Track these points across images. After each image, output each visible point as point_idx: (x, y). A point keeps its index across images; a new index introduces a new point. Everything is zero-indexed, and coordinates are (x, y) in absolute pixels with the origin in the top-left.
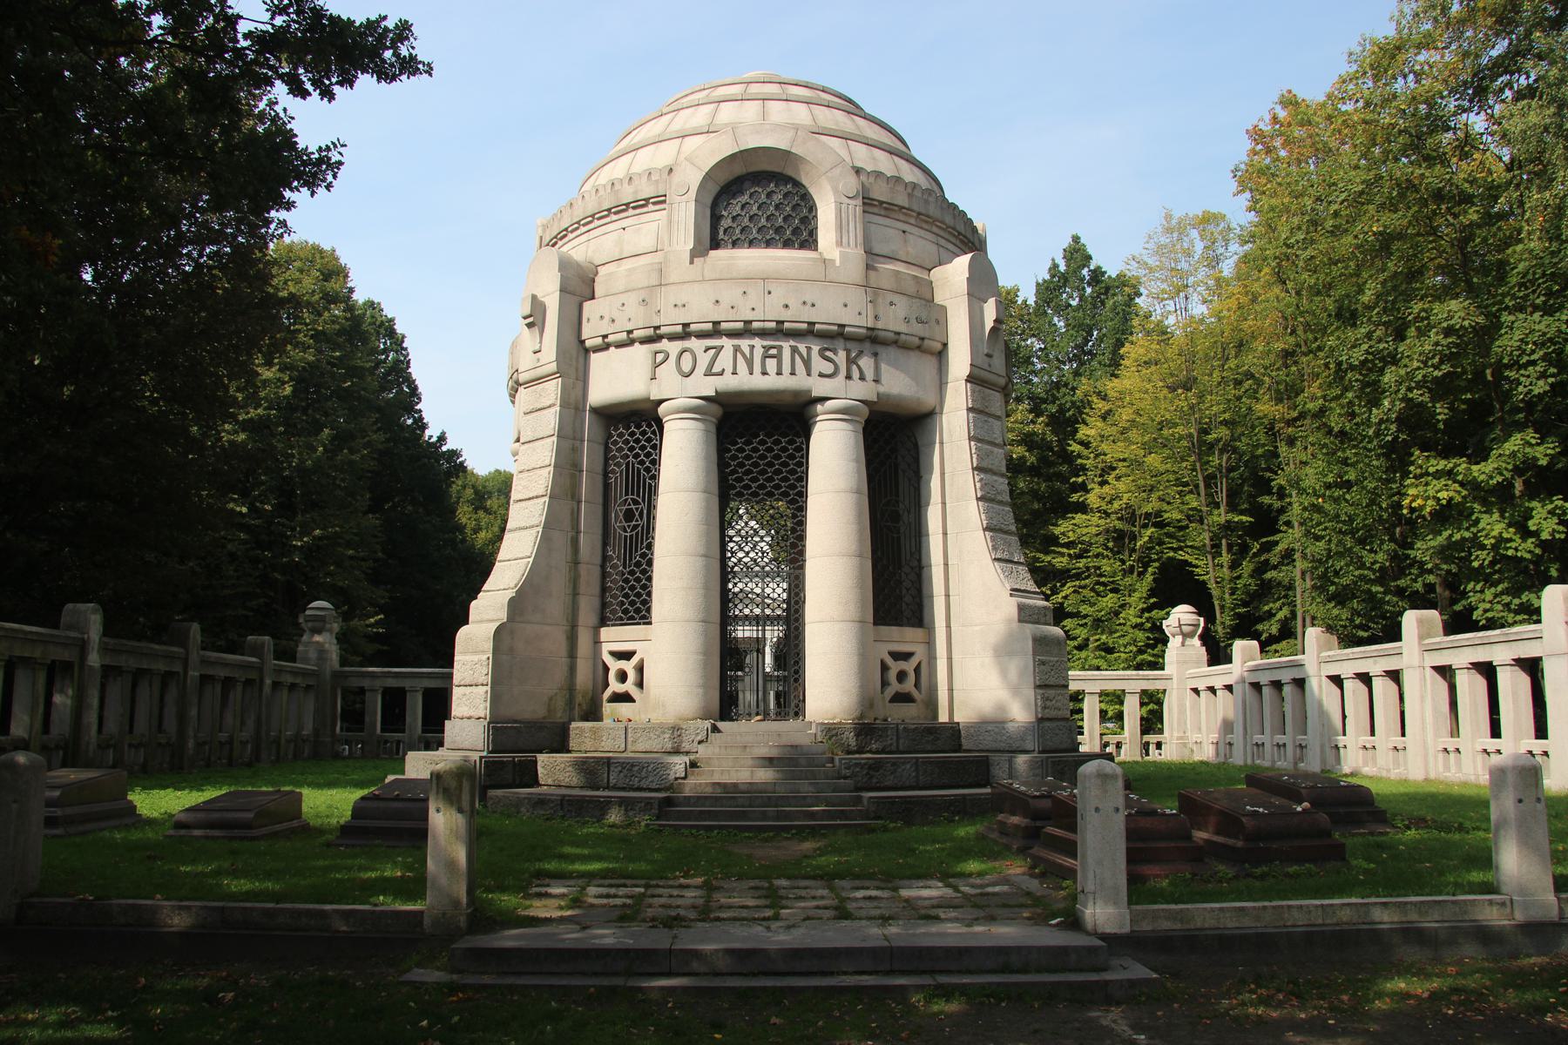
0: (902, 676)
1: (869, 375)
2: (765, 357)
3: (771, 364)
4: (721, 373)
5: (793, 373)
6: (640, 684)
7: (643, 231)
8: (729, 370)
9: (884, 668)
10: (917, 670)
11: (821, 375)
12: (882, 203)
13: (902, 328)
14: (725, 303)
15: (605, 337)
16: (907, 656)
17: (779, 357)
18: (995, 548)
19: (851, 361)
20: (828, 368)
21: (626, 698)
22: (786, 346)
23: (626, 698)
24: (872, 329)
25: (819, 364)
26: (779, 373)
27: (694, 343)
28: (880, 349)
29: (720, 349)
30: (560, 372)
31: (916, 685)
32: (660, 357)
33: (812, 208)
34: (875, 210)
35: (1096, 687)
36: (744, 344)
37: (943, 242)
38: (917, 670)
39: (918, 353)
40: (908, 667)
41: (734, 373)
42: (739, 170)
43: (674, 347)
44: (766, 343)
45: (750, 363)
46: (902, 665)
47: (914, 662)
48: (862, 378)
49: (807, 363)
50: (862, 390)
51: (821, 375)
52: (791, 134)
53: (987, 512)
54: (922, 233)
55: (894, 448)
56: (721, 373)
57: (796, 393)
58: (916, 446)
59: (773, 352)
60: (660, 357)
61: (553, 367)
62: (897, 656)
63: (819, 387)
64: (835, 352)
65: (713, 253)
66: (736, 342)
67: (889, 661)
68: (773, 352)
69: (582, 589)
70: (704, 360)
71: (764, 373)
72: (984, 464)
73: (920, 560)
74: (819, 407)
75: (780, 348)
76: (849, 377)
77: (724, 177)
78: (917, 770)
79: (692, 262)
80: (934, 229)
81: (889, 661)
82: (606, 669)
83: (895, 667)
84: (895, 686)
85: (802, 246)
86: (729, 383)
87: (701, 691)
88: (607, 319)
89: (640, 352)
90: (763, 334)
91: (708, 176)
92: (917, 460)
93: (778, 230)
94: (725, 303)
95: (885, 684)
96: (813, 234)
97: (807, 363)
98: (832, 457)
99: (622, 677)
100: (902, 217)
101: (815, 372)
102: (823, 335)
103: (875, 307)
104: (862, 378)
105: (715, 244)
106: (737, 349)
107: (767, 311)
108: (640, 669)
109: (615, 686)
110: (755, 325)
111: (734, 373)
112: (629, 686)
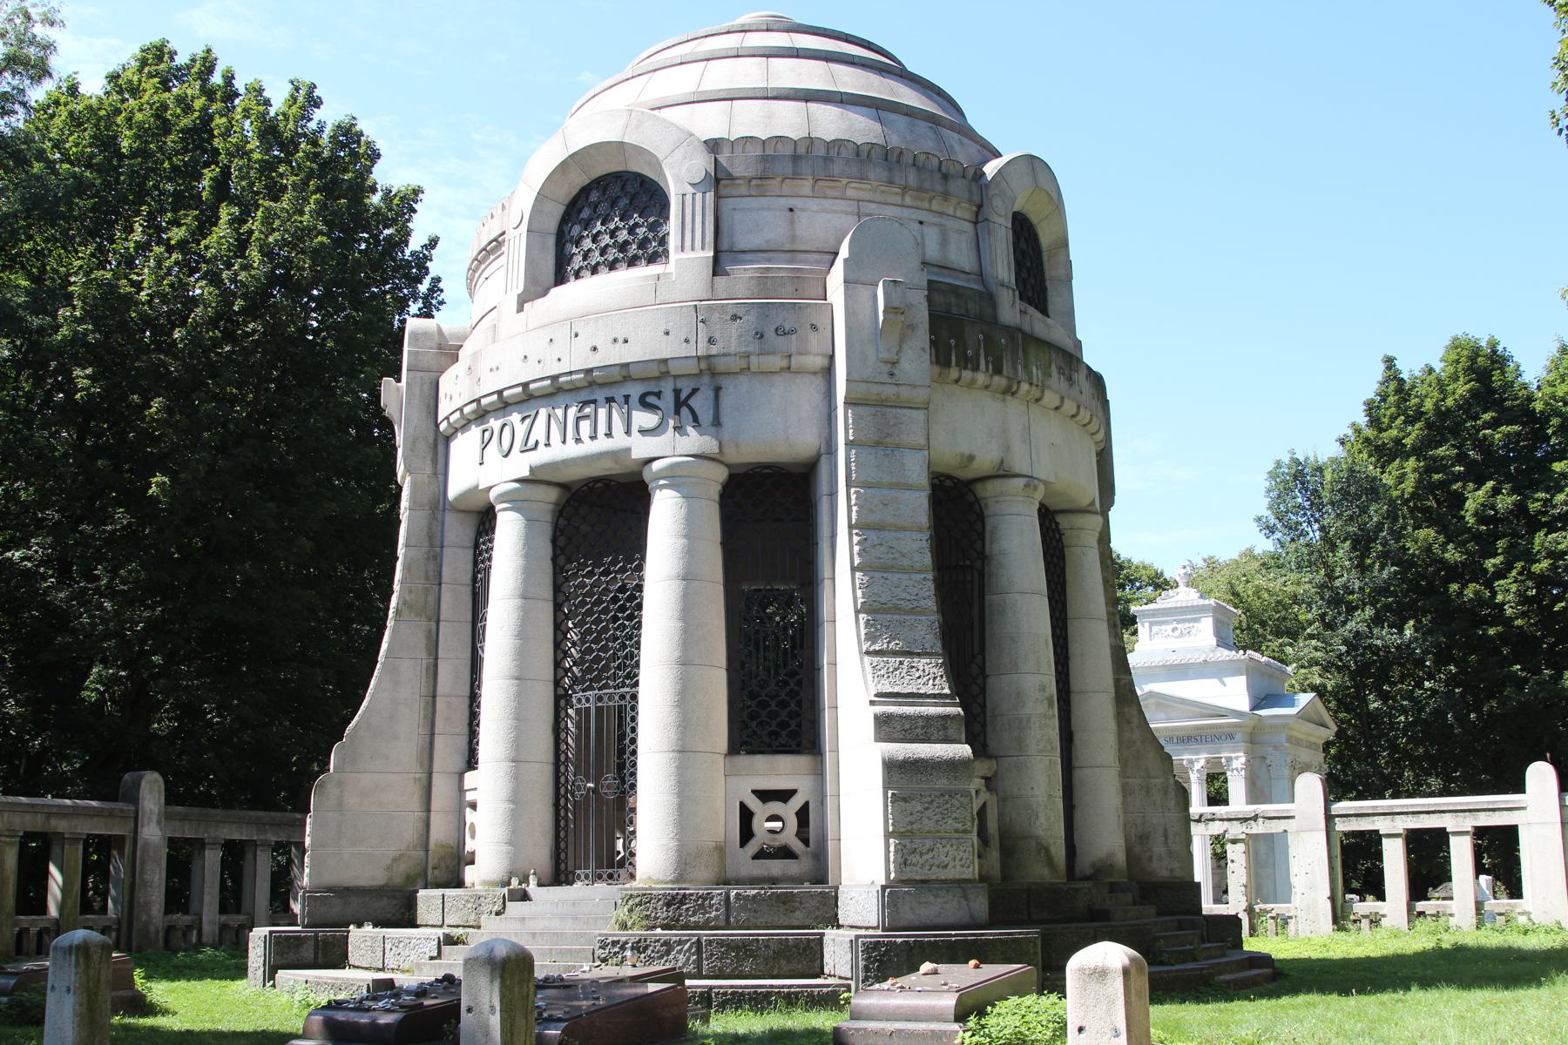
1: (706, 416)
3: (585, 426)
5: (609, 435)
8: (542, 441)
9: (746, 815)
11: (643, 432)
14: (532, 360)
16: (785, 796)
18: (871, 637)
24: (709, 357)
32: (487, 434)
35: (1468, 823)
38: (803, 814)
39: (787, 375)
42: (579, 180)
43: (495, 424)
47: (796, 803)
51: (643, 432)
53: (866, 587)
54: (827, 203)
55: (767, 518)
60: (487, 434)
62: (765, 796)
63: (641, 447)
64: (658, 395)
65: (555, 291)
67: (754, 804)
69: (439, 726)
70: (521, 430)
71: (578, 440)
72: (875, 518)
78: (699, 952)
79: (520, 309)
81: (754, 804)
85: (652, 259)
87: (505, 848)
89: (475, 432)
91: (541, 196)
93: (623, 247)
95: (746, 834)
96: (663, 241)
101: (635, 428)
102: (574, 389)
105: (560, 279)
107: (573, 359)
111: (547, 445)
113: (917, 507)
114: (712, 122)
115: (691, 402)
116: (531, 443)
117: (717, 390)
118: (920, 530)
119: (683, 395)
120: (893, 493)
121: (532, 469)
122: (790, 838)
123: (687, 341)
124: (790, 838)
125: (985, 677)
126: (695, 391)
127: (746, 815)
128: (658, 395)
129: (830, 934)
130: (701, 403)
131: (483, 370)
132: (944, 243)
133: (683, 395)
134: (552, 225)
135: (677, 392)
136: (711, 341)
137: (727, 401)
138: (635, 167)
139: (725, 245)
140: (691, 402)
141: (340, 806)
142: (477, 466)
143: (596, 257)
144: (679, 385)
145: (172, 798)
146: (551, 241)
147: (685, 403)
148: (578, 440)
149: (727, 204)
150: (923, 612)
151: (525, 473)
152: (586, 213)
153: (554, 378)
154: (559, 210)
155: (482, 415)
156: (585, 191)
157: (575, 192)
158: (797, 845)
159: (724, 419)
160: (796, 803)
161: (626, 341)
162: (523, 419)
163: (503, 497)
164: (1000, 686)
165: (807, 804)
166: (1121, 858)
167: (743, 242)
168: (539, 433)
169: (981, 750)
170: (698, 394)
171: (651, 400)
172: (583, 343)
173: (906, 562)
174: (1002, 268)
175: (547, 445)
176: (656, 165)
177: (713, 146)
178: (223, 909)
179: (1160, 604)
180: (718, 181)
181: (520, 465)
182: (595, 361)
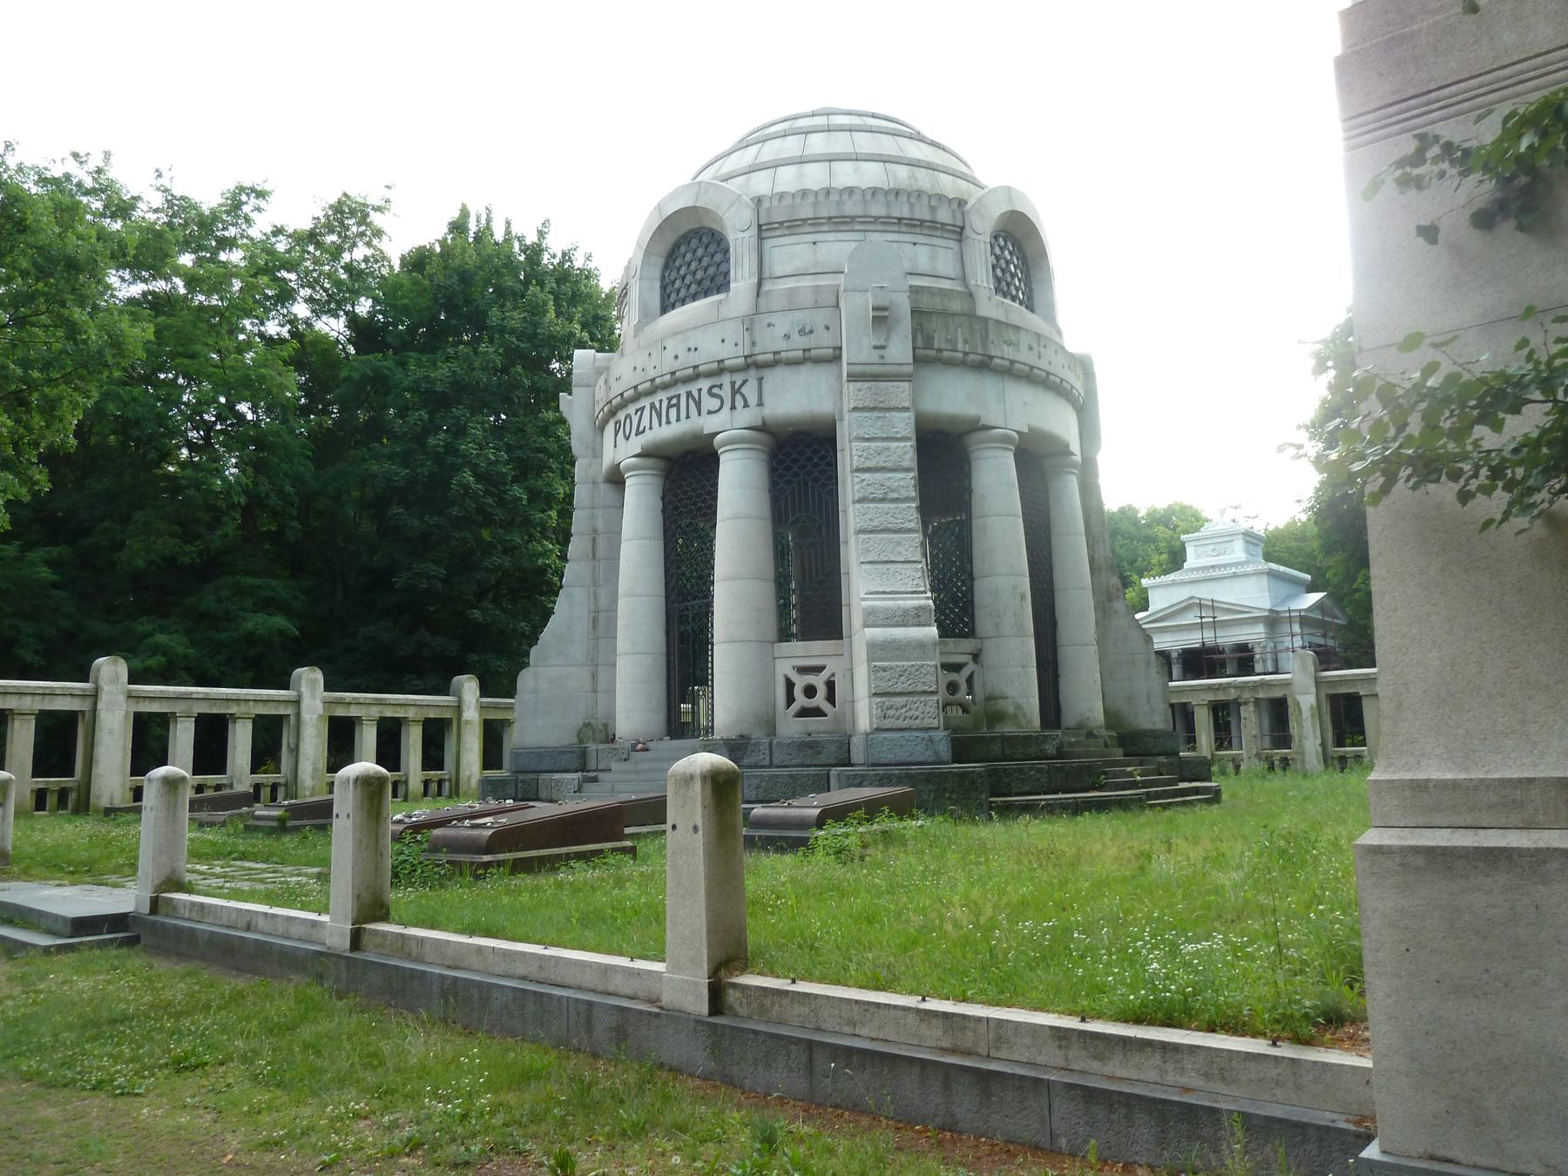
0: (810, 691)
3: (673, 411)
9: (790, 685)
11: (710, 412)
12: (781, 223)
13: (781, 345)
14: (639, 369)
17: (678, 405)
20: (715, 403)
22: (682, 390)
25: (709, 403)
26: (678, 420)
28: (767, 373)
31: (831, 698)
34: (778, 233)
42: (671, 238)
43: (621, 416)
48: (746, 405)
50: (746, 417)
51: (710, 412)
54: (840, 236)
59: (674, 401)
63: (709, 424)
64: (720, 386)
67: (795, 677)
68: (674, 401)
70: (635, 420)
71: (668, 422)
76: (733, 407)
77: (663, 248)
80: (858, 227)
84: (801, 700)
86: (649, 437)
90: (665, 387)
93: (700, 283)
94: (639, 369)
95: (790, 699)
97: (698, 405)
98: (738, 487)
101: (704, 411)
104: (746, 405)
110: (658, 381)
113: (905, 452)
114: (761, 184)
117: (761, 380)
118: (907, 470)
120: (882, 444)
122: (819, 700)
124: (819, 700)
125: (972, 579)
126: (745, 381)
127: (790, 685)
128: (720, 386)
129: (834, 771)
130: (750, 391)
131: (612, 381)
132: (933, 258)
134: (657, 274)
135: (733, 384)
136: (753, 344)
137: (767, 387)
139: (766, 274)
141: (535, 690)
142: (620, 450)
143: (683, 293)
145: (485, 691)
146: (657, 285)
148: (668, 422)
149: (768, 244)
150: (909, 531)
152: (677, 264)
153: (653, 380)
154: (660, 262)
155: (613, 413)
156: (677, 246)
157: (669, 247)
158: (826, 706)
159: (766, 400)
160: (825, 675)
164: (984, 589)
166: (1099, 716)
167: (779, 270)
168: (645, 422)
169: (945, 632)
171: (715, 390)
172: (669, 354)
173: (895, 495)
174: (982, 278)
176: (719, 220)
177: (759, 201)
178: (487, 765)
180: (763, 231)
181: (636, 444)
182: (676, 365)
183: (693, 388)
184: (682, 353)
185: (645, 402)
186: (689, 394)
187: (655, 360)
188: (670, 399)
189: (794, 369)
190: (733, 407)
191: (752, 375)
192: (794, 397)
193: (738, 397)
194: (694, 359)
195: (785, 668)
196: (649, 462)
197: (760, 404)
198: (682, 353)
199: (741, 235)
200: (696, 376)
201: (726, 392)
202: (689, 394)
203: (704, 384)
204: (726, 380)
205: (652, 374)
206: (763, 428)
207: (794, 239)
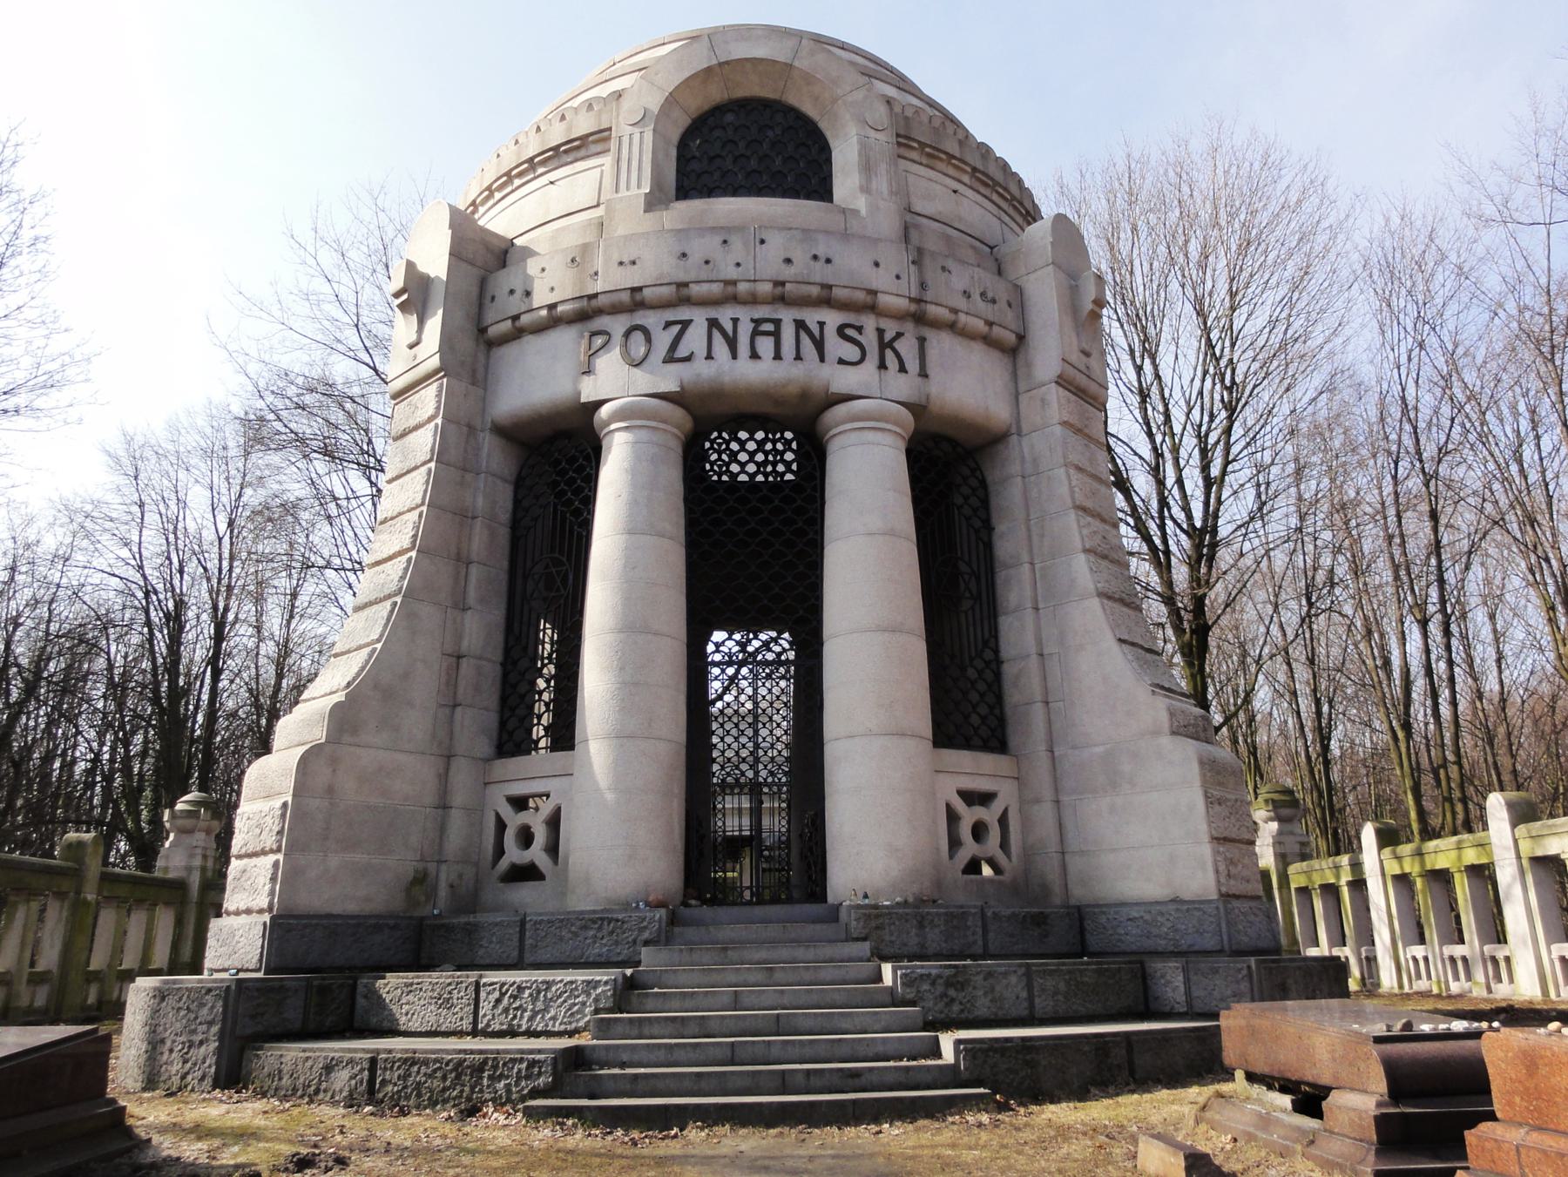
0: (979, 831)
1: (912, 365)
2: (756, 333)
3: (765, 345)
4: (688, 359)
5: (798, 357)
6: (553, 849)
7: (579, 184)
9: (952, 817)
10: (1003, 820)
11: (841, 362)
12: (922, 145)
15: (516, 318)
16: (984, 799)
17: (776, 335)
19: (884, 345)
20: (852, 352)
21: (528, 873)
22: (787, 316)
23: (528, 873)
26: (778, 356)
27: (652, 319)
28: (929, 333)
29: (685, 324)
30: (444, 369)
31: (1004, 845)
33: (825, 149)
34: (914, 155)
36: (725, 315)
37: (1007, 219)
38: (1003, 820)
40: (989, 815)
41: (709, 357)
42: (717, 94)
43: (617, 325)
44: (756, 316)
45: (732, 343)
46: (980, 813)
47: (997, 807)
49: (819, 345)
51: (841, 362)
52: (791, 43)
56: (688, 359)
57: (804, 395)
58: (983, 484)
59: (769, 327)
61: (435, 362)
63: (844, 380)
64: (859, 329)
66: (712, 313)
70: (663, 340)
71: (755, 355)
73: (996, 651)
74: (841, 410)
75: (777, 323)
76: (882, 366)
80: (995, 197)
82: (501, 826)
83: (969, 816)
86: (701, 371)
88: (519, 293)
91: (672, 100)
92: (985, 503)
94: (696, 256)
95: (955, 843)
97: (819, 345)
99: (526, 837)
100: (951, 171)
103: (921, 272)
106: (713, 324)
108: (554, 822)
109: (514, 854)
110: (743, 287)
112: (536, 853)
115: (896, 345)
116: (682, 352)
117: (922, 341)
119: (888, 337)
121: (682, 387)
123: (898, 277)
126: (899, 335)
130: (907, 347)
133: (888, 337)
135: (881, 332)
136: (923, 286)
138: (792, 99)
140: (896, 345)
144: (882, 326)
147: (890, 345)
148: (755, 355)
151: (670, 386)
156: (718, 110)
157: (706, 107)
161: (828, 261)
162: (668, 324)
163: (620, 415)
165: (1005, 812)
170: (902, 339)
171: (850, 332)
175: (709, 357)
179: (1409, 619)
182: (788, 273)
183: (812, 317)
184: (800, 256)
185: (699, 317)
186: (800, 325)
187: (738, 249)
188: (757, 322)
189: (965, 342)
190: (882, 366)
191: (909, 328)
192: (966, 385)
193: (889, 353)
194: (820, 273)
195: (948, 790)
196: (677, 413)
197: (924, 374)
198: (800, 256)
199: (872, 134)
200: (826, 300)
201: (870, 339)
202: (800, 325)
203: (833, 319)
204: (869, 323)
205: (731, 273)
206: (917, 409)
207: (932, 174)
